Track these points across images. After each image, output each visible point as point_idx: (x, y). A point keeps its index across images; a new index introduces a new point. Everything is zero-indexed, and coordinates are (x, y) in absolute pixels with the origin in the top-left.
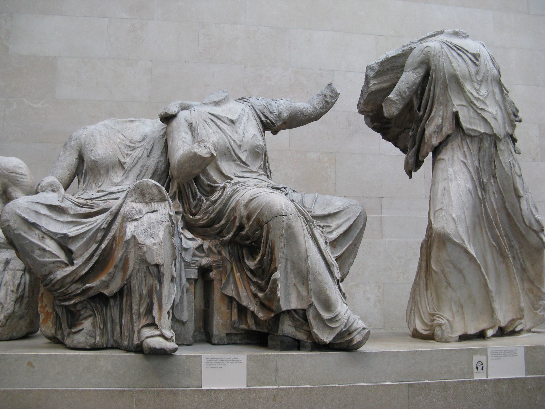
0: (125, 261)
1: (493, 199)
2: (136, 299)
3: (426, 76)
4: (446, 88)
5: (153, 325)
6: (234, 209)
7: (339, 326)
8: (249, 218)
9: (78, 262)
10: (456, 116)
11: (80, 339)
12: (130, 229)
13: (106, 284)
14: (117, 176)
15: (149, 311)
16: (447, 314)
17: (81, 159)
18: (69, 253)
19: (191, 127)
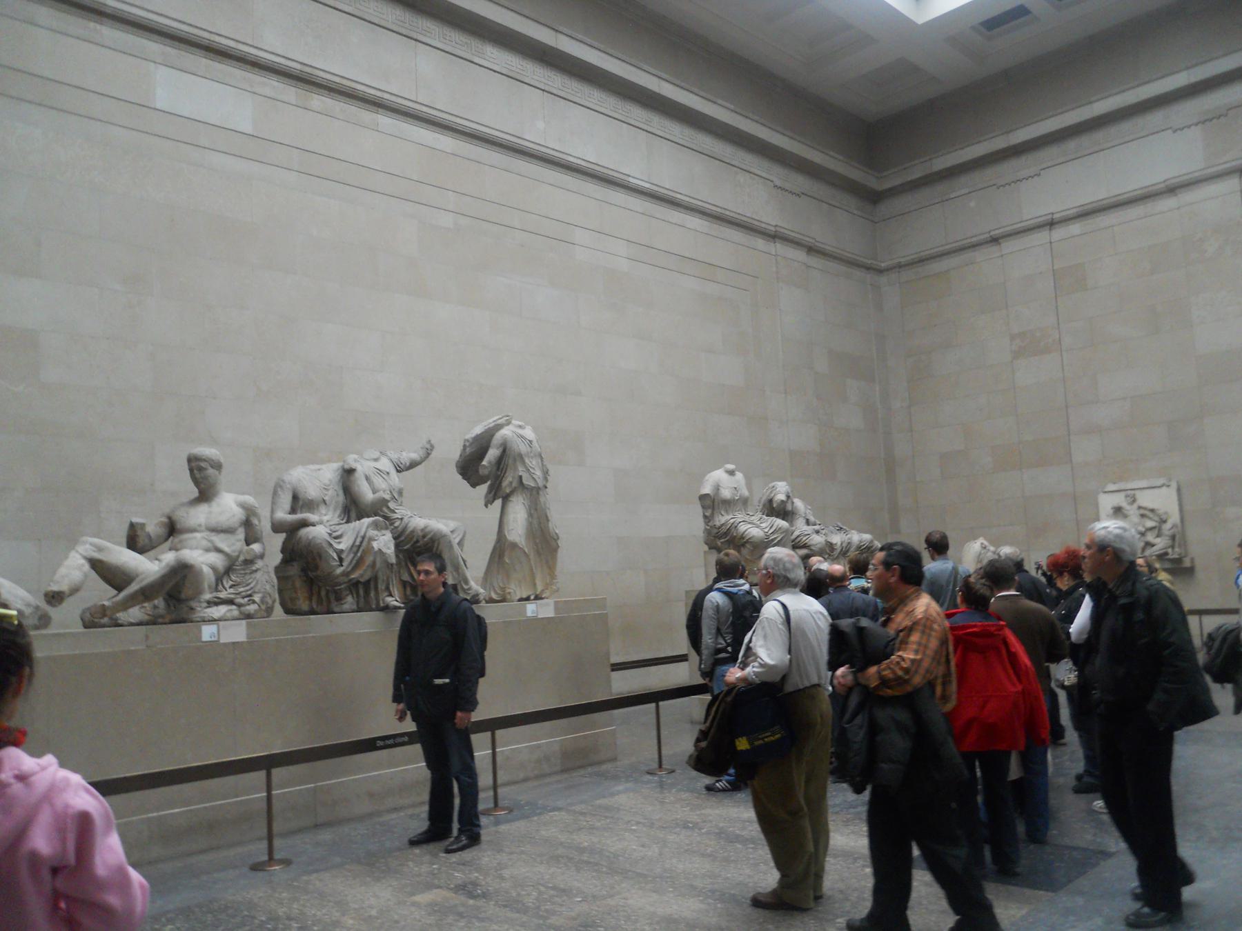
0: (374, 563)
1: (535, 522)
2: (380, 582)
3: (504, 451)
4: (515, 460)
5: (391, 595)
6: (413, 532)
7: (472, 592)
8: (424, 537)
9: (345, 564)
10: (521, 477)
11: (346, 607)
12: (375, 545)
13: (362, 576)
14: (323, 509)
15: (388, 588)
16: (513, 586)
17: (295, 498)
18: (341, 560)
19: (367, 478)
